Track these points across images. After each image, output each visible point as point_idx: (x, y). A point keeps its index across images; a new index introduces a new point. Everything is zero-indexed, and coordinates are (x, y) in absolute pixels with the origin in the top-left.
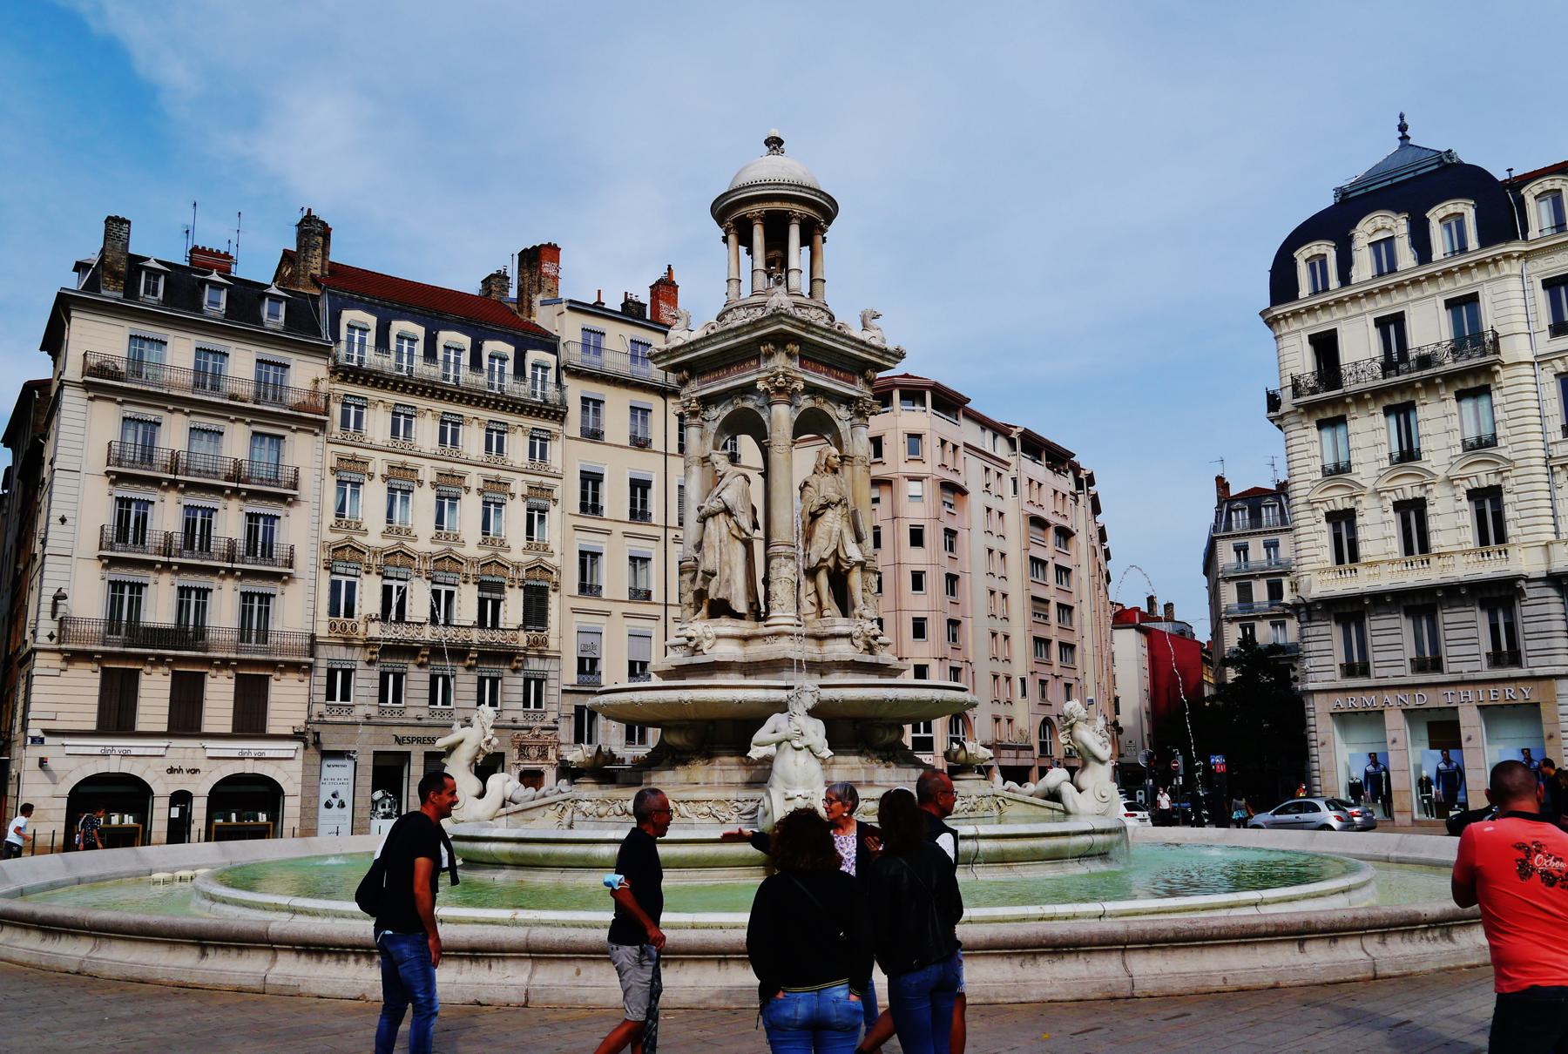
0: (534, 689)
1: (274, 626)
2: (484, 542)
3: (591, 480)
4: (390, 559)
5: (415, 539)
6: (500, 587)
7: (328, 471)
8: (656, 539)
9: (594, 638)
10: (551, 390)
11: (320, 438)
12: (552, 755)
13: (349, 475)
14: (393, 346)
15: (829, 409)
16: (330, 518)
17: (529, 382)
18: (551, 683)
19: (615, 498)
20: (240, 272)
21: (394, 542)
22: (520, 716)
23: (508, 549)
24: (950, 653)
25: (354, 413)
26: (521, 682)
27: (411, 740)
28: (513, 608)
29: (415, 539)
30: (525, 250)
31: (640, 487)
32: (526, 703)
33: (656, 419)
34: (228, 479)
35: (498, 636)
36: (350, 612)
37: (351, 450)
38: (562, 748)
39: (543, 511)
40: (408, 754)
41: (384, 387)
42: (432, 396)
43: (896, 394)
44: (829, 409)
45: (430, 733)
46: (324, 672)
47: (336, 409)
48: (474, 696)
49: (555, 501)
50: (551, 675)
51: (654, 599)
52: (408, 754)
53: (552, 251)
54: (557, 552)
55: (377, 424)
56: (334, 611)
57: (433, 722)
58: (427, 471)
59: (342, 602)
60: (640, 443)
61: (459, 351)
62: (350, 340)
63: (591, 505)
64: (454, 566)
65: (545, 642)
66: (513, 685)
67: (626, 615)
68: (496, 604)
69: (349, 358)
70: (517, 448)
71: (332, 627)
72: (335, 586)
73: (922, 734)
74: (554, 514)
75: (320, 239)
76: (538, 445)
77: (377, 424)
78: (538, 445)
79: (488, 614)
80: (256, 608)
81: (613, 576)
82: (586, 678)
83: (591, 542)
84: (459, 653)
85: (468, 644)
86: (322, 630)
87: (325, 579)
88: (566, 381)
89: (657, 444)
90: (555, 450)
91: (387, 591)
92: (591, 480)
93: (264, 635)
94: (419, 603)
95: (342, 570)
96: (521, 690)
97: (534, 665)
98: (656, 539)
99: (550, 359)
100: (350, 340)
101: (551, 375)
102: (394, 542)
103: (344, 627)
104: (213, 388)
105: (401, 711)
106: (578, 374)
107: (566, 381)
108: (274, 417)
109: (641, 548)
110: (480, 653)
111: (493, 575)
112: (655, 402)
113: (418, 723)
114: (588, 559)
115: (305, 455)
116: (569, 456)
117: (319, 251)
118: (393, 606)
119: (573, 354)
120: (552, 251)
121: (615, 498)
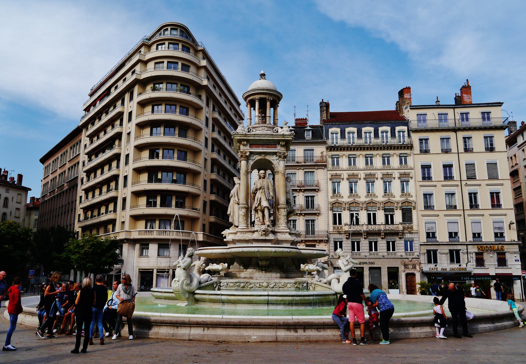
0: (409, 245)
1: (316, 229)
2: (385, 195)
3: (426, 168)
4: (352, 205)
5: (360, 197)
6: (392, 210)
7: (329, 180)
8: (457, 186)
9: (433, 225)
10: (406, 138)
11: (325, 170)
12: (418, 267)
13: (336, 180)
14: (347, 137)
15: (268, 157)
16: (331, 194)
17: (397, 138)
18: (415, 242)
19: (437, 173)
20: (310, 123)
21: (352, 199)
22: (404, 254)
23: (394, 196)
25: (336, 160)
26: (403, 242)
27: (364, 263)
28: (398, 217)
29: (360, 197)
30: (399, 92)
31: (448, 167)
32: (406, 249)
33: (453, 142)
34: (298, 187)
35: (391, 227)
36: (340, 223)
37: (335, 172)
38: (422, 265)
39: (408, 182)
40: (363, 268)
41: (344, 150)
42: (361, 150)
44: (268, 157)
45: (372, 261)
46: (333, 243)
47: (330, 160)
48: (386, 248)
49: (412, 178)
50: (415, 239)
51: (458, 208)
52: (363, 268)
53: (408, 89)
54: (414, 195)
55: (344, 162)
56: (335, 223)
57: (371, 257)
58: (379, 174)
59: (337, 219)
60: (446, 151)
61: (370, 133)
62: (333, 138)
63: (427, 177)
64: (374, 205)
65: (412, 228)
66: (400, 244)
67: (446, 215)
68: (392, 216)
69: (333, 143)
70: (395, 162)
71: (334, 228)
72: (335, 215)
74: (412, 182)
75: (325, 108)
76: (403, 159)
77: (344, 162)
78: (403, 159)
79: (389, 219)
80: (310, 225)
81: (439, 201)
82: (453, 239)
83: (428, 190)
84: (377, 233)
85: (380, 231)
86: (331, 229)
87: (331, 214)
88: (412, 135)
89: (454, 150)
90: (410, 160)
91: (369, 215)
92: (426, 168)
93: (313, 232)
94: (363, 217)
95: (336, 210)
96: (403, 245)
97: (408, 236)
98: (457, 186)
99: (405, 128)
100: (333, 138)
101: (406, 134)
102: (352, 199)
103: (338, 228)
104: (292, 161)
105: (395, 254)
106: (416, 131)
107: (412, 135)
108: (311, 166)
110: (385, 233)
112: (452, 135)
113: (365, 257)
114: (427, 196)
115: (321, 176)
116: (415, 161)
117: (325, 112)
118: (355, 220)
119: (414, 125)
120: (408, 89)
121: (437, 173)
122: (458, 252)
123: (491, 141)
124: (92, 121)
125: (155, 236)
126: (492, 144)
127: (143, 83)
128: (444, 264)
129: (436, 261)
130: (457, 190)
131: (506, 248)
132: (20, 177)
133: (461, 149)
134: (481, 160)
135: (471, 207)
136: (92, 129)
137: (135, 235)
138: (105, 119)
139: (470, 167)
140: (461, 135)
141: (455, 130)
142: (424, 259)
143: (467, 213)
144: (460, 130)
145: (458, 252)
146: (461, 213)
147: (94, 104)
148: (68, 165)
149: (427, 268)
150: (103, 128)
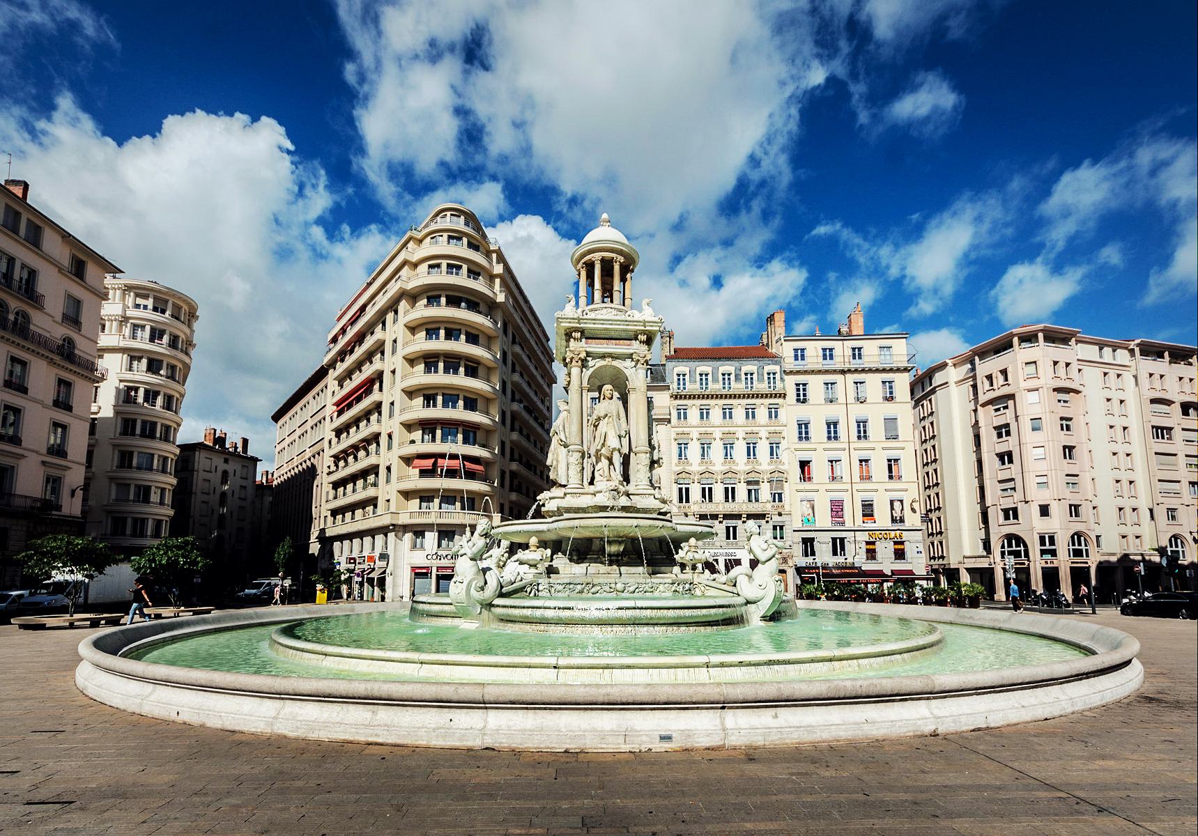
0: (779, 529)
19: (818, 431)
24: (1068, 495)
33: (839, 388)
36: (687, 501)
43: (1016, 340)
51: (844, 480)
73: (1048, 547)
74: (783, 445)
76: (773, 413)
78: (773, 413)
79: (752, 495)
81: (819, 470)
88: (786, 377)
89: (842, 399)
99: (776, 368)
106: (791, 373)
109: (834, 455)
111: (753, 477)
112: (839, 378)
121: (818, 431)
122: (842, 540)
123: (891, 387)
124: (342, 355)
125: (432, 519)
126: (891, 393)
127: (412, 297)
128: (823, 556)
129: (813, 554)
130: (843, 456)
131: (905, 535)
132: (245, 442)
133: (851, 399)
134: (876, 413)
135: (862, 478)
136: (341, 367)
137: (404, 519)
138: (359, 352)
139: (862, 425)
140: (851, 378)
141: (843, 372)
142: (798, 549)
143: (855, 487)
144: (849, 371)
145: (842, 540)
146: (848, 487)
147: (343, 331)
148: (311, 423)
149: (803, 561)
150: (358, 366)
